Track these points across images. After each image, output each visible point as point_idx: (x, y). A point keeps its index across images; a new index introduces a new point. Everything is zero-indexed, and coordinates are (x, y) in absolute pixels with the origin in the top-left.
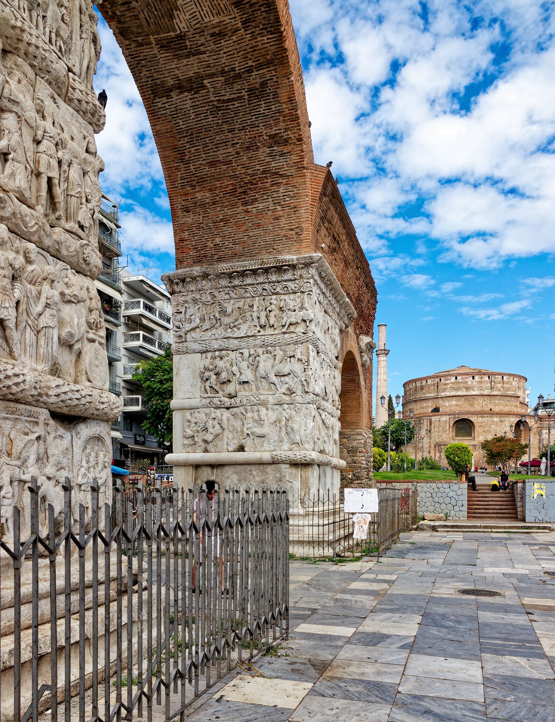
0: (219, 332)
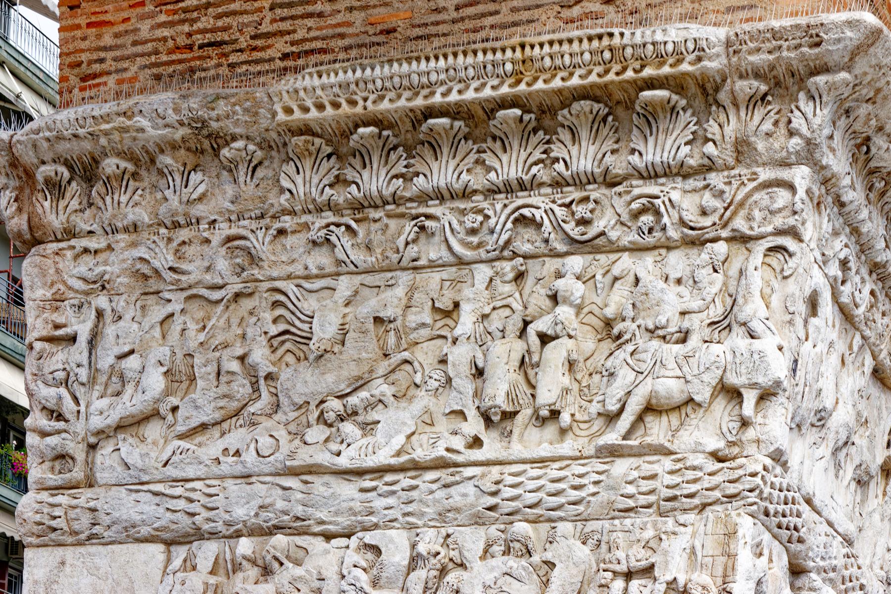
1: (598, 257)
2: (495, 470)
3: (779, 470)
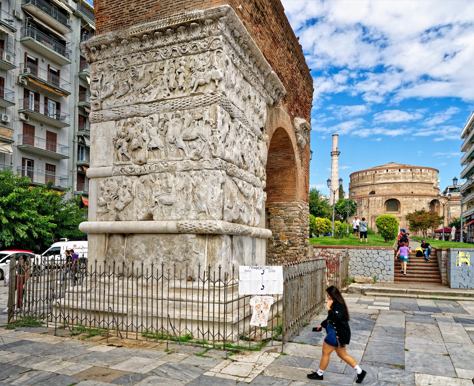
0: (132, 98)
2: (173, 100)
3: (224, 96)
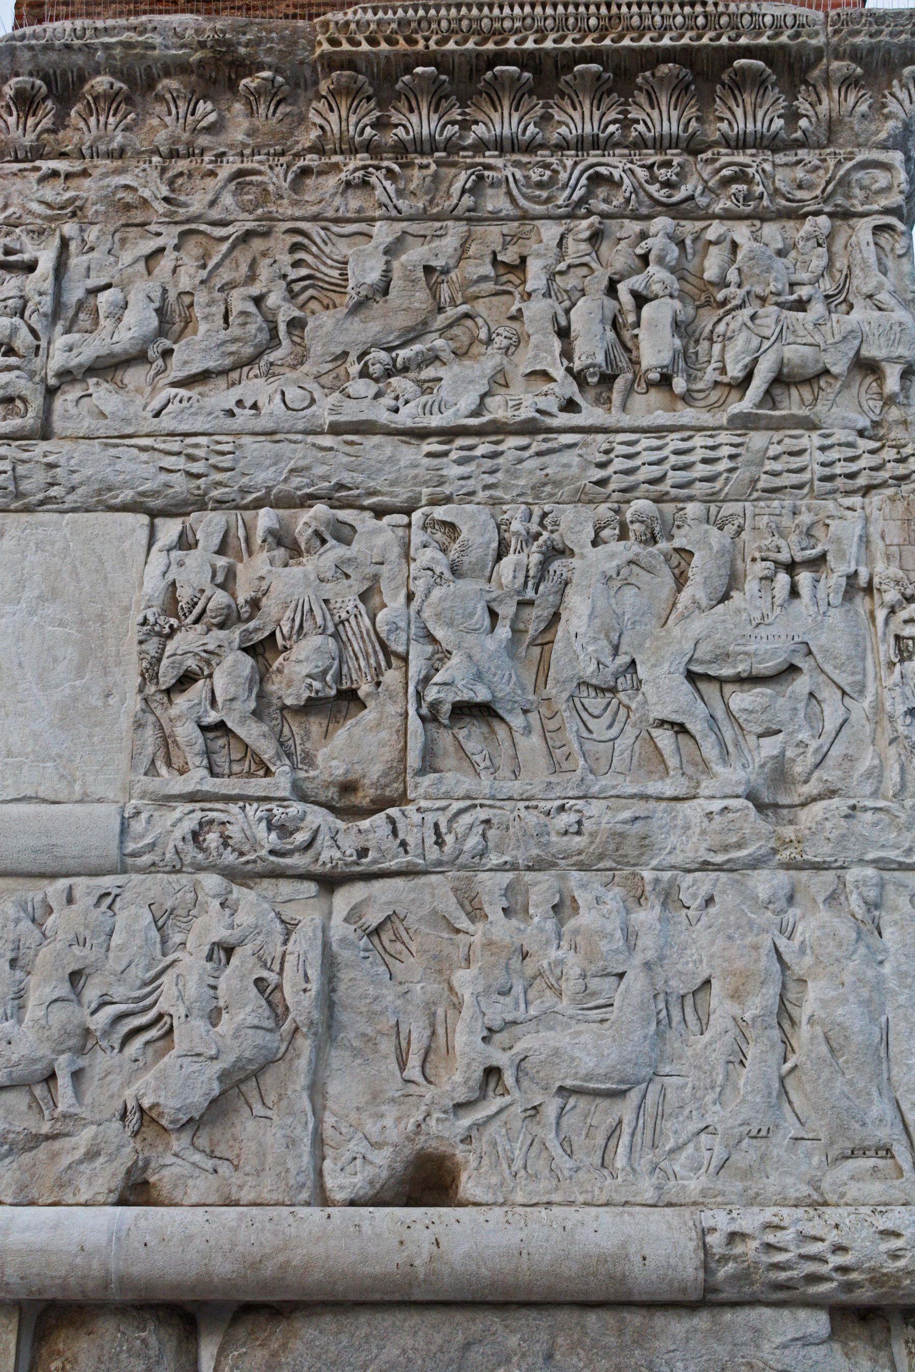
1: (683, 223)
